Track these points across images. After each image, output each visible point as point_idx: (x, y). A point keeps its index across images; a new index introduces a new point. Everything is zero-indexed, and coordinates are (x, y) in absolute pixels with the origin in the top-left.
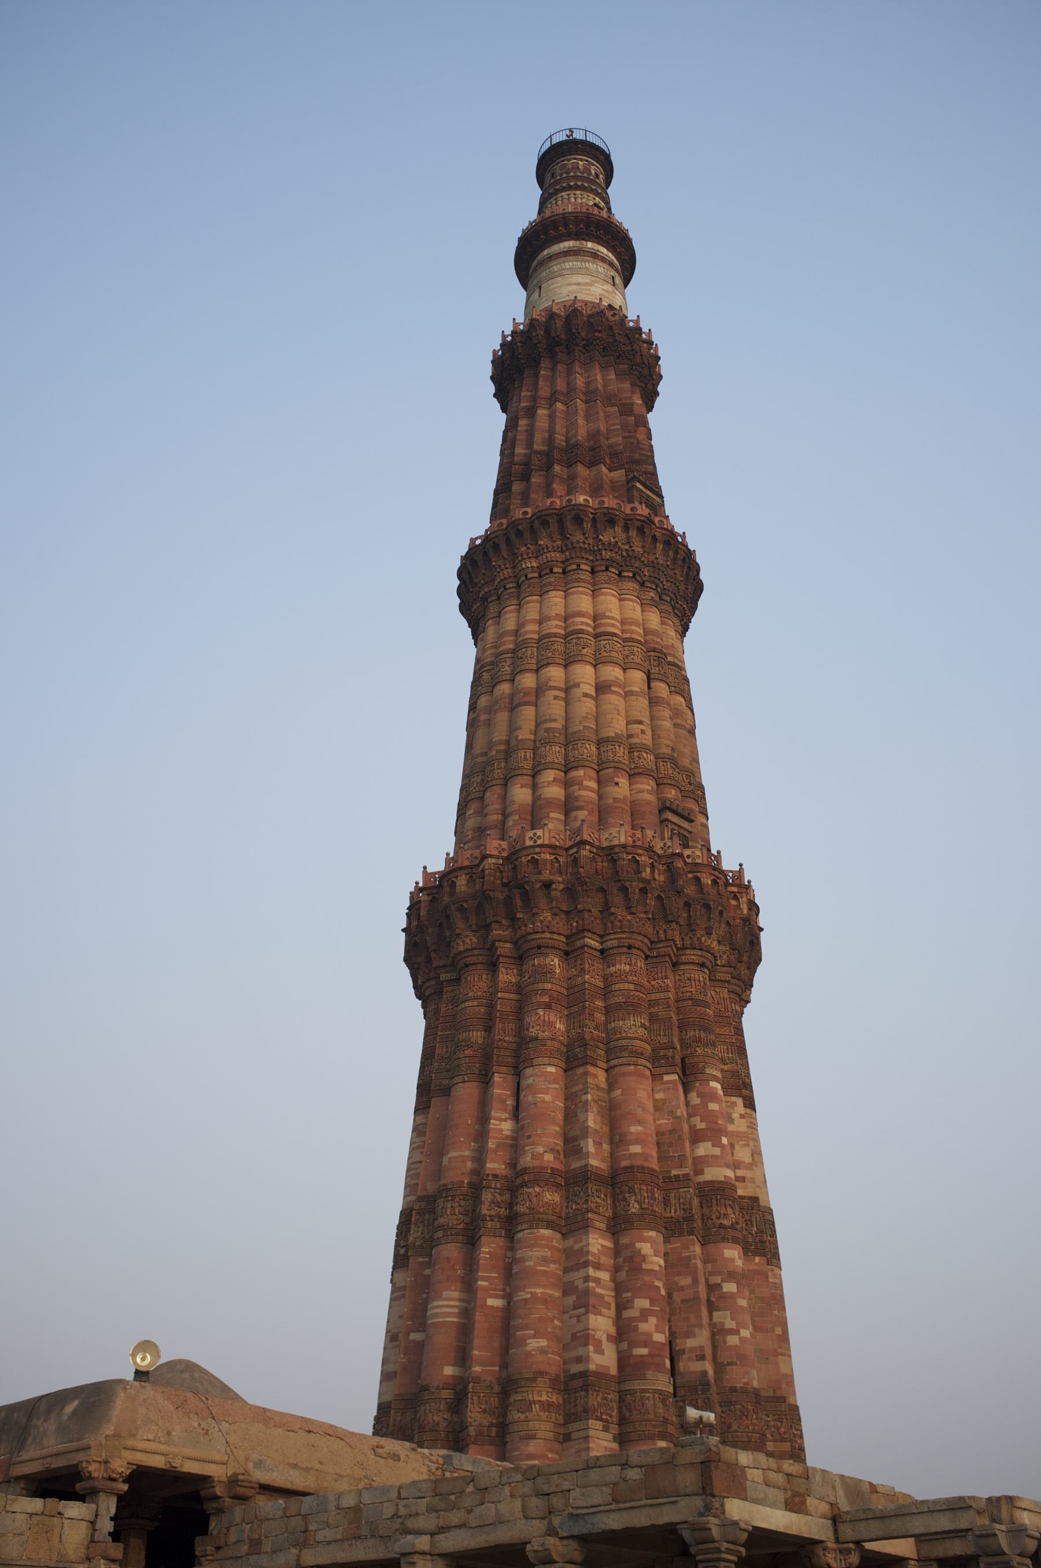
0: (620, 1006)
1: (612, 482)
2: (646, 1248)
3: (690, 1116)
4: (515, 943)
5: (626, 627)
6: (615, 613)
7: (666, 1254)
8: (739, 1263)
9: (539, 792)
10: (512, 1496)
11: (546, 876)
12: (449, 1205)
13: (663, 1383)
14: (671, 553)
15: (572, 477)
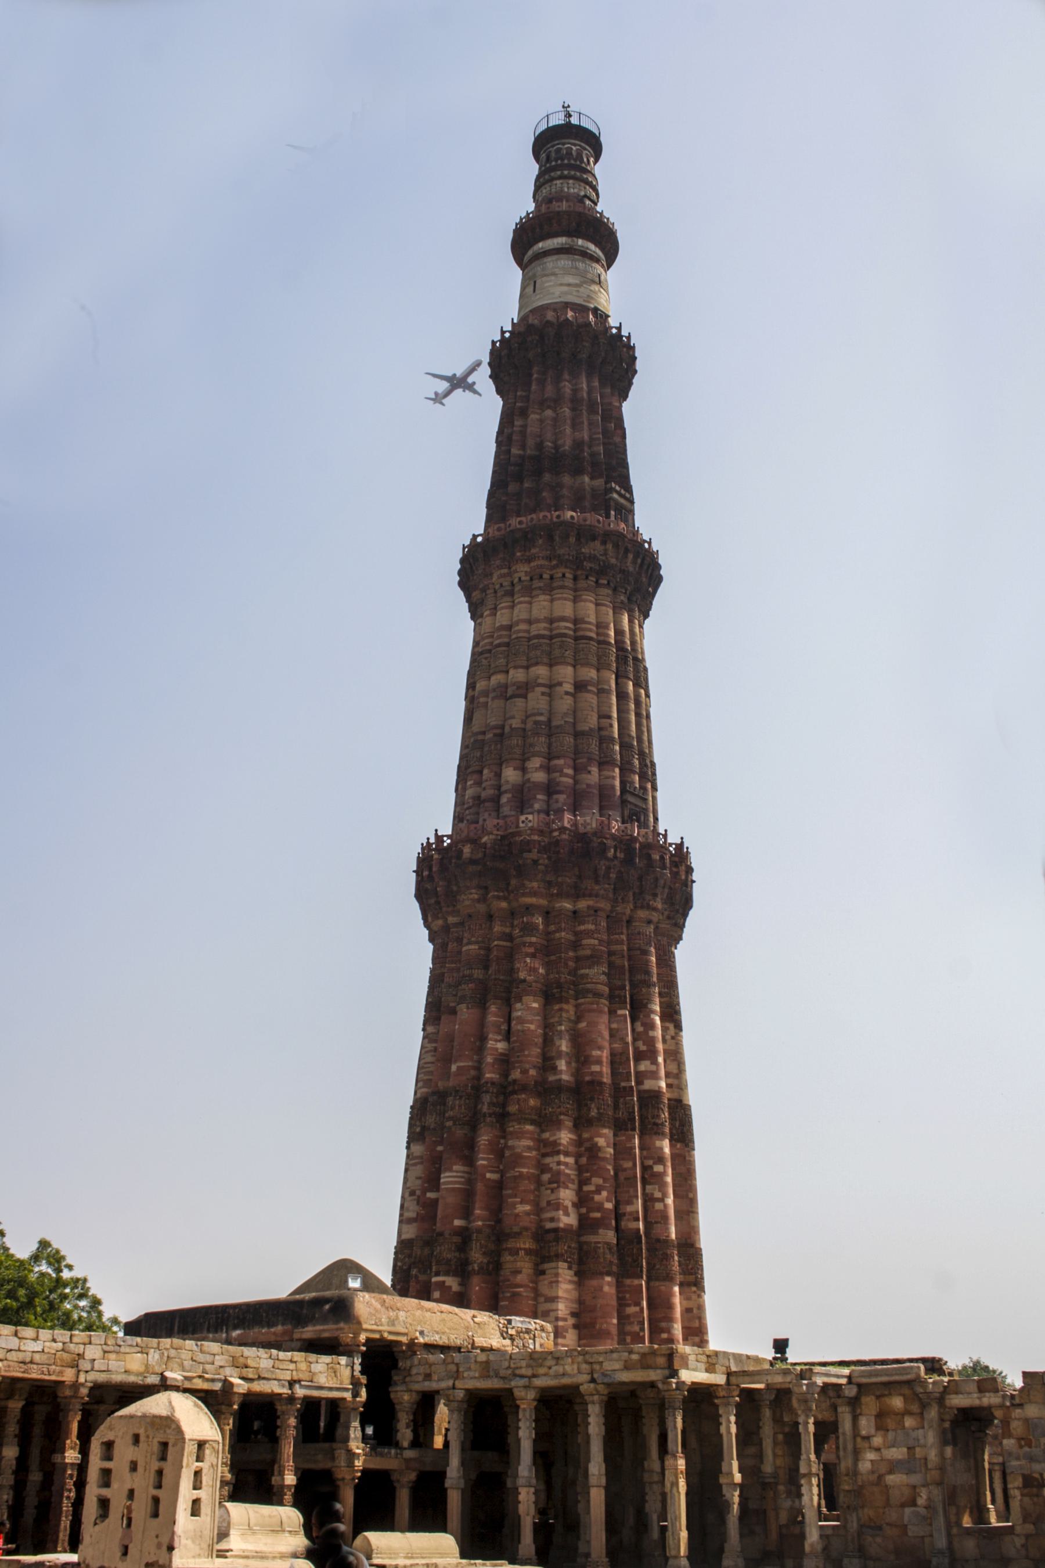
0: (588, 958)
1: (593, 490)
2: (601, 1142)
3: (634, 1040)
4: (509, 903)
5: (601, 631)
6: (592, 619)
7: (615, 1144)
8: (667, 1150)
9: (527, 776)
10: (573, 1362)
11: (534, 855)
12: (457, 1102)
13: (610, 1236)
14: (639, 561)
15: (560, 485)
